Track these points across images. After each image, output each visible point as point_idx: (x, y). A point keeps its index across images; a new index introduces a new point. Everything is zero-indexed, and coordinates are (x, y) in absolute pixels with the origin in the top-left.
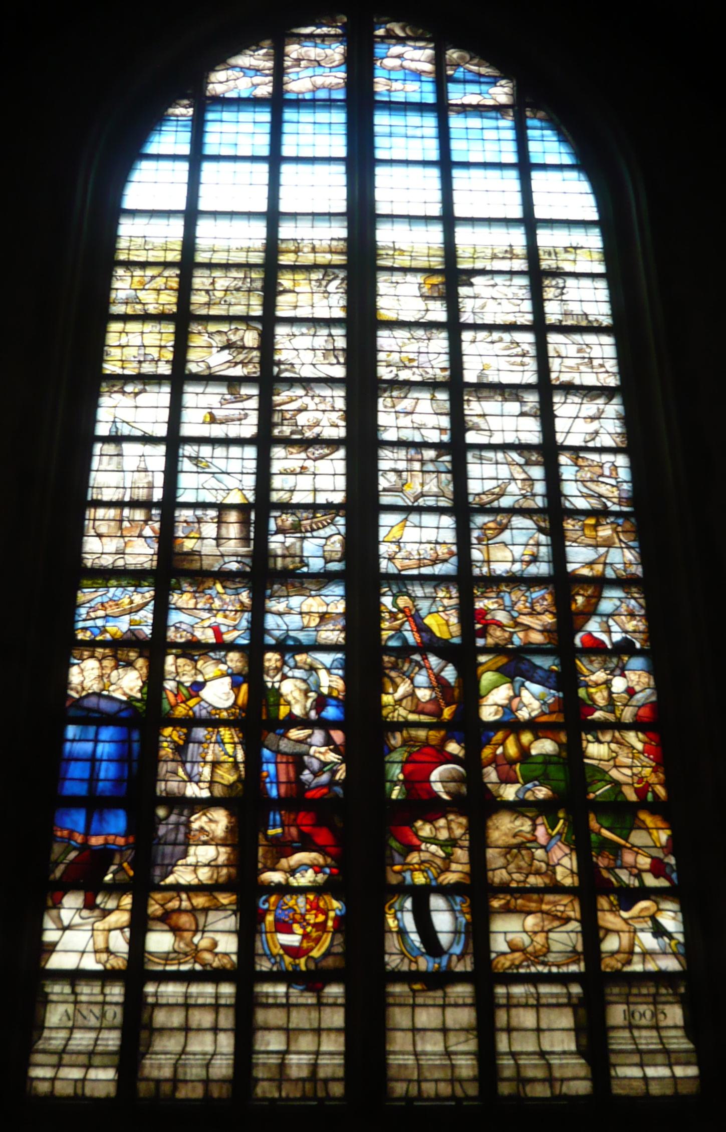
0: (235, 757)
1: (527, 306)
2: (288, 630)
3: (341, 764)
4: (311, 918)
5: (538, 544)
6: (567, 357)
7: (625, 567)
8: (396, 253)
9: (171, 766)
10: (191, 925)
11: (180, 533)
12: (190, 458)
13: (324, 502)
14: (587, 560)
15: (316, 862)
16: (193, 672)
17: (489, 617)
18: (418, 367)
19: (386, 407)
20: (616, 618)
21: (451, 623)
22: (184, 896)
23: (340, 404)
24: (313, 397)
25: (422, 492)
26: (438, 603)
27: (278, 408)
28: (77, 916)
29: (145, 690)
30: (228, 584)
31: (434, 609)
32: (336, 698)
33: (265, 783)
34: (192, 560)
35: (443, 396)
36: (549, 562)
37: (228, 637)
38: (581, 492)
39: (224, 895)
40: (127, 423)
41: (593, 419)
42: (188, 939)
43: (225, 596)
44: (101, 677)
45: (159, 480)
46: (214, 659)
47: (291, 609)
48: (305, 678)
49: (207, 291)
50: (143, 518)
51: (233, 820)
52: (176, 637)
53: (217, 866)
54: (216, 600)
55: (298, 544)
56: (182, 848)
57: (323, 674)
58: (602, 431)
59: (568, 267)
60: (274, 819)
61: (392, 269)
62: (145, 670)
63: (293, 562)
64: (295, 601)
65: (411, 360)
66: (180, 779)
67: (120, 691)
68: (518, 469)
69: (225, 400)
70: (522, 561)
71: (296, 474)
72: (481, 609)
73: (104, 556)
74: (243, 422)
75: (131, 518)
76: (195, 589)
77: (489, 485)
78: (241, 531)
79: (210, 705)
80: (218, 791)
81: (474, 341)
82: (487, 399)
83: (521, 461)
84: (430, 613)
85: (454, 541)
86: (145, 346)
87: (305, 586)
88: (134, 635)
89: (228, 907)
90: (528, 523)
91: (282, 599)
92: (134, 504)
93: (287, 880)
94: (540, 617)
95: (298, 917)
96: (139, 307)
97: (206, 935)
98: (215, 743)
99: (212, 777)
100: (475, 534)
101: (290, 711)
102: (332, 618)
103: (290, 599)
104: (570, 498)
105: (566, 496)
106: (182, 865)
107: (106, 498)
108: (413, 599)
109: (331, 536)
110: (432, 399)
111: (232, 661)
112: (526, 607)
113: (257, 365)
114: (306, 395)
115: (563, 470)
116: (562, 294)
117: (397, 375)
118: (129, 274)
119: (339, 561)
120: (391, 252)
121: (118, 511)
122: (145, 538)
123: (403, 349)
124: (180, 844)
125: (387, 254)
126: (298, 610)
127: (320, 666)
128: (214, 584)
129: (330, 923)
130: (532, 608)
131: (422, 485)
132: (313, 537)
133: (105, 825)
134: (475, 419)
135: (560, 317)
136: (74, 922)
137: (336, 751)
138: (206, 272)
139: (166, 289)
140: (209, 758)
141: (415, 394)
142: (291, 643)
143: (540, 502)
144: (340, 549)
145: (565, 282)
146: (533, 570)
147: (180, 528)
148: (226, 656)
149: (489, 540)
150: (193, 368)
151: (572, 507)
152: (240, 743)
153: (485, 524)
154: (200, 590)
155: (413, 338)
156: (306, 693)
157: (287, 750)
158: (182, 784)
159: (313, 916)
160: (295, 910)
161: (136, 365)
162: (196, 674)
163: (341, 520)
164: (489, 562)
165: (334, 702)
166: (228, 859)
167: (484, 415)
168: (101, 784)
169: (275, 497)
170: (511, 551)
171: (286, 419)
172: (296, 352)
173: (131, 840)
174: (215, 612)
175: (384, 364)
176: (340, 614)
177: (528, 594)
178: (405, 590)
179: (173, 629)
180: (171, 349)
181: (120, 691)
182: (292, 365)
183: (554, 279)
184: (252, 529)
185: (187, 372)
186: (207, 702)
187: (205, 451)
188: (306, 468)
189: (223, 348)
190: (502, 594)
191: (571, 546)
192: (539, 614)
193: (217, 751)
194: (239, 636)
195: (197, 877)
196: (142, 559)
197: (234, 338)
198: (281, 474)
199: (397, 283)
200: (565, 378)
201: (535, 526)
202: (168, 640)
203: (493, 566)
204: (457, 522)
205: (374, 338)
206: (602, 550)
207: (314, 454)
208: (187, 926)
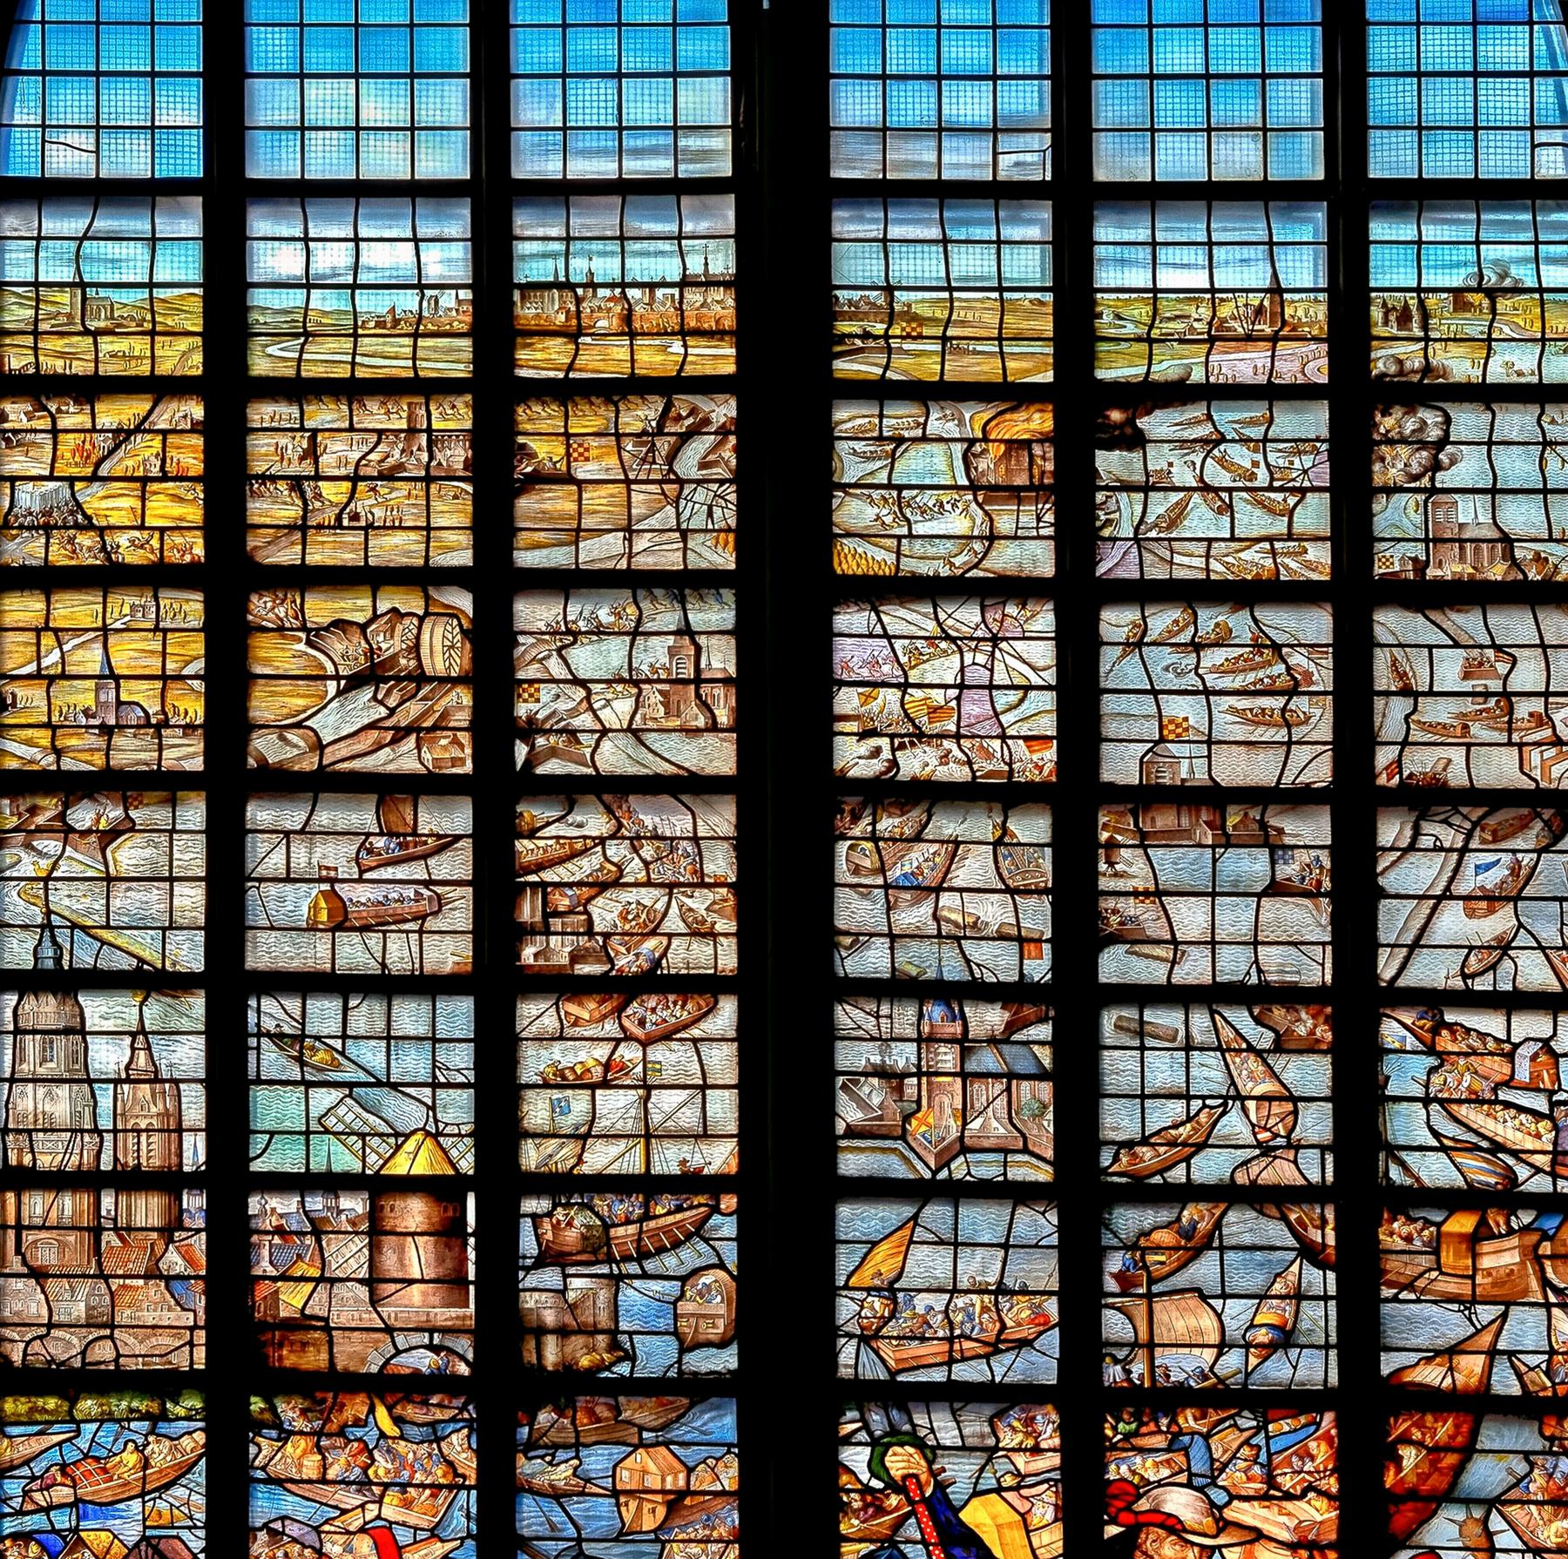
1: (1314, 514)
2: (579, 1540)
5: (1298, 1296)
6: (1431, 693)
7: (1549, 1362)
8: (895, 330)
11: (264, 1266)
12: (278, 1037)
13: (675, 1169)
14: (1441, 1343)
17: (1143, 1505)
18: (958, 737)
19: (856, 870)
20: (1508, 1510)
21: (1035, 1521)
23: (720, 863)
24: (635, 842)
25: (962, 1138)
26: (1001, 1465)
27: (533, 878)
30: (410, 1411)
31: (988, 1481)
34: (304, 1345)
35: (1033, 828)
36: (1327, 1347)
38: (1436, 1134)
40: (84, 928)
41: (1492, 900)
43: (402, 1447)
45: (194, 1106)
47: (588, 1481)
49: (296, 483)
50: (155, 1221)
54: (376, 1454)
55: (604, 1295)
58: (1523, 939)
59: (1460, 366)
61: (880, 391)
64: (597, 1460)
65: (935, 711)
68: (1253, 1063)
69: (370, 851)
70: (1247, 1346)
71: (593, 1087)
72: (1123, 1480)
73: (55, 1333)
74: (431, 924)
75: (122, 1222)
76: (317, 1424)
77: (1165, 1114)
78: (440, 1260)
81: (1136, 644)
82: (1171, 838)
83: (1265, 1039)
84: (976, 1494)
85: (1055, 1286)
86: (117, 678)
88: (156, 1550)
90: (1277, 1232)
91: (561, 1455)
92: (130, 1180)
94: (1289, 1505)
96: (86, 540)
100: (1115, 1263)
102: (700, 1507)
103: (583, 1452)
104: (1403, 1155)
105: (1393, 1151)
107: (45, 1162)
108: (931, 1452)
109: (696, 1272)
110: (998, 843)
112: (1249, 1479)
113: (465, 738)
114: (613, 837)
115: (1390, 1065)
116: (1436, 466)
117: (894, 763)
118: (45, 423)
119: (722, 1344)
120: (879, 329)
121: (85, 1200)
122: (168, 1279)
123: (914, 677)
125: (866, 336)
126: (608, 1483)
128: (372, 1410)
130: (1270, 1481)
131: (964, 1116)
132: (645, 1276)
134: (1130, 907)
135: (1418, 550)
138: (285, 412)
139: (165, 478)
141: (947, 825)
143: (1314, 1169)
144: (722, 1310)
145: (1448, 421)
146: (1278, 1371)
147: (265, 1252)
149: (1152, 1281)
150: (266, 747)
151: (1409, 1181)
153: (1146, 1234)
155: (948, 638)
161: (94, 740)
163: (727, 1227)
164: (1151, 1346)
167: (1158, 894)
169: (531, 1156)
170: (1219, 1316)
171: (557, 914)
172: (582, 693)
174: (377, 1490)
175: (852, 727)
176: (723, 1493)
177: (1260, 1440)
178: (907, 1427)
179: (263, 1536)
180: (198, 685)
182: (572, 734)
183: (1411, 410)
184: (471, 1254)
185: (252, 762)
187: (324, 1013)
188: (622, 1067)
189: (355, 682)
190: (1186, 1439)
191: (1395, 1299)
192: (1288, 1496)
196: (166, 1341)
197: (390, 644)
198: (546, 1085)
199: (900, 440)
200: (1420, 762)
201: (1292, 1242)
203: (1163, 1357)
204: (1061, 1229)
205: (826, 637)
206: (1486, 1313)
207: (642, 1023)
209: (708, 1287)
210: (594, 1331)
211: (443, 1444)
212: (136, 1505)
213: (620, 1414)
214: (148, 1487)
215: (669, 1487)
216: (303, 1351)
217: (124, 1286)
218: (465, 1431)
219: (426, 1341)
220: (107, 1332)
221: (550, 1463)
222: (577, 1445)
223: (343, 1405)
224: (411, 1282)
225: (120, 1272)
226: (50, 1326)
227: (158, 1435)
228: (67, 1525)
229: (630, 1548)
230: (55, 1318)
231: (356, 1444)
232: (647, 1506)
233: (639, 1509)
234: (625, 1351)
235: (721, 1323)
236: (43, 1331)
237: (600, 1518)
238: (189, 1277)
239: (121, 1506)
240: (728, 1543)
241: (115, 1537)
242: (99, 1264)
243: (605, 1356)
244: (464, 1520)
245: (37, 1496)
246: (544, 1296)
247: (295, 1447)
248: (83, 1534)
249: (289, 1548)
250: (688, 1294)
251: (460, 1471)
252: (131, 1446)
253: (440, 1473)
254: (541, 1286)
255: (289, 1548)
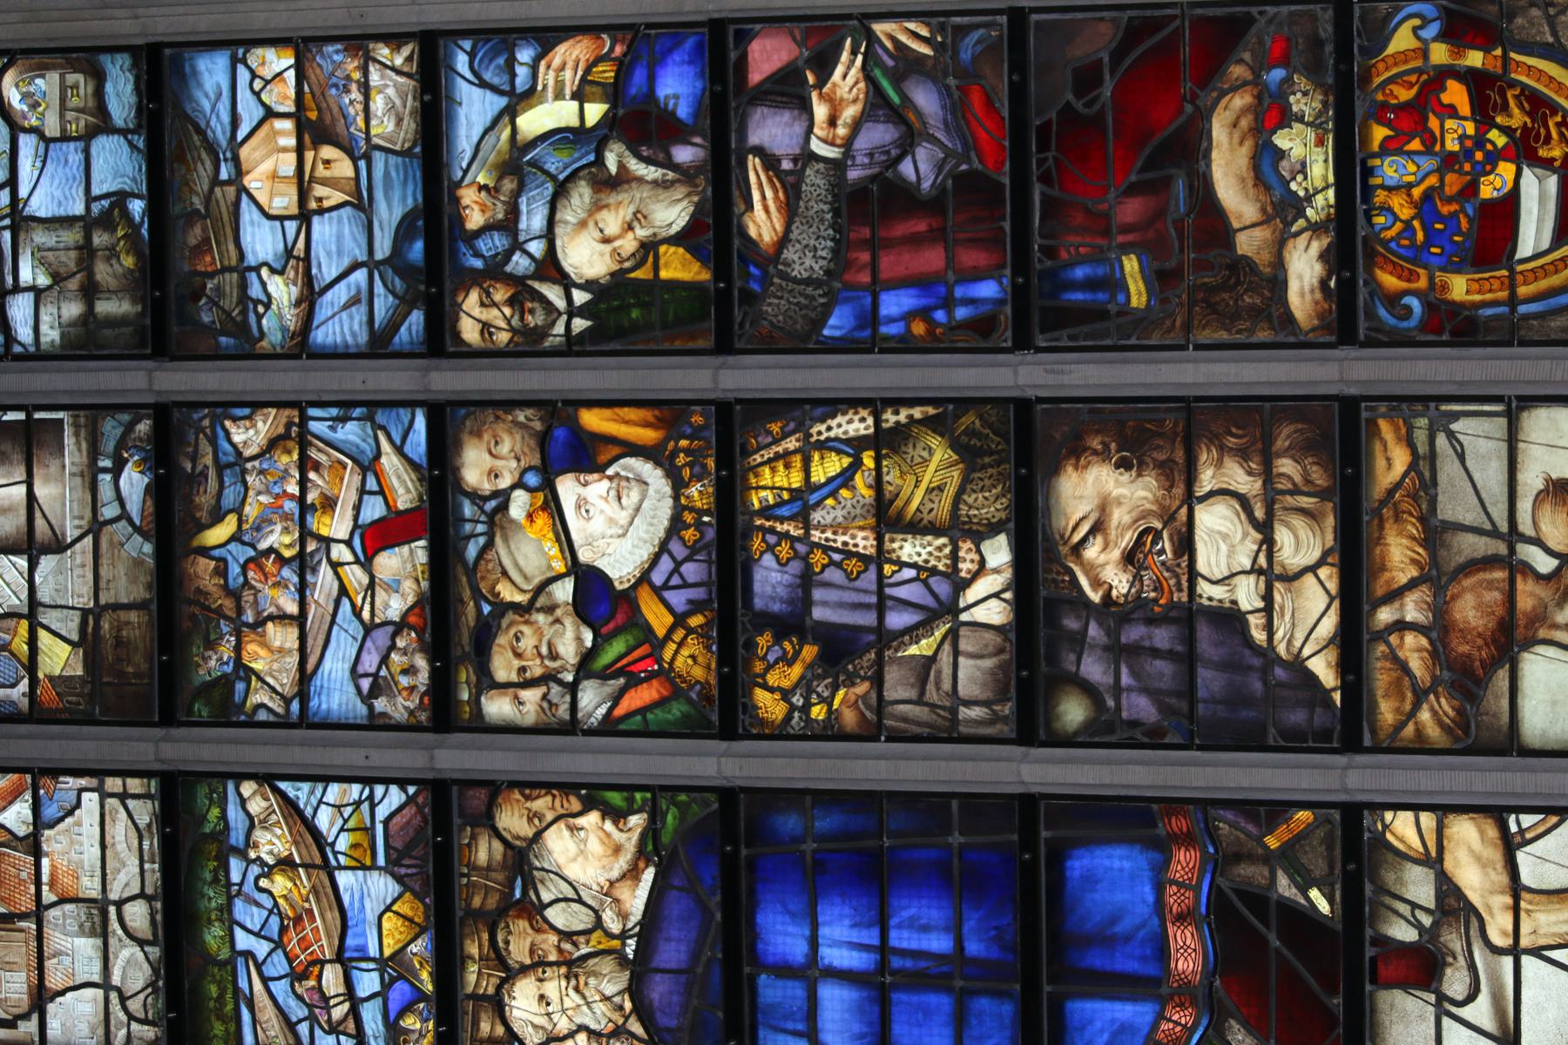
0: (856, 445)
2: (371, 264)
3: (871, 38)
4: (1454, 133)
9: (897, 686)
10: (1490, 585)
15: (1245, 123)
16: (541, 618)
22: (1385, 615)
28: (1466, 1012)
29: (615, 798)
30: (205, 500)
32: (624, 68)
33: (955, 327)
34: (119, 642)
37: (405, 492)
39: (1380, 463)
42: (1543, 592)
43: (251, 511)
44: (572, 967)
46: (490, 544)
47: (289, 252)
48: (549, 188)
51: (1096, 443)
52: (412, 689)
53: (1271, 496)
54: (263, 545)
55: (41, 237)
56: (1204, 632)
57: (534, 121)
60: (1091, 284)
62: (541, 804)
63: (112, 253)
64: (261, 241)
66: (947, 647)
67: (623, 892)
73: (116, 979)
76: (225, 627)
79: (663, 548)
80: (988, 504)
87: (198, 203)
89: (1422, 449)
91: (255, 291)
93: (1316, 228)
95: (1453, 182)
97: (1525, 526)
98: (807, 526)
99: (934, 530)
101: (677, 240)
102: (320, 97)
103: (251, 260)
106: (1269, 628)
111: (494, 474)
119: (99, 77)
122: (39, 822)
124: (1190, 640)
126: (291, 226)
127: (506, 134)
128: (205, 551)
129: (1475, 59)
133: (1120, 928)
136: (1488, 1024)
137: (824, 64)
140: (864, 542)
142: (417, 250)
144: (54, 77)
148: (476, 497)
152: (802, 428)
154: (228, 604)
156: (608, 184)
157: (825, 248)
158: (964, 645)
159: (1450, 124)
160: (1428, 196)
162: (550, 609)
165: (639, 77)
166: (1243, 455)
168: (973, 947)
173: (1179, 824)
176: (299, 67)
179: (380, 704)
181: (623, 892)
186: (655, 560)
193: (839, 514)
194: (399, 450)
195: (1312, 569)
196: (120, 830)
202: (423, 717)
208: (1495, 596)
209: (25, 96)
210: (86, 251)
211: (248, 453)
212: (343, 879)
213: (198, 211)
214: (318, 861)
215: (291, 142)
216: (129, 642)
217: (52, 884)
218: (227, 423)
219: (108, 477)
220: (112, 909)
221: (268, 306)
222: (243, 270)
223: (199, 591)
224: (31, 496)
225: (32, 889)
226: (105, 985)
227: (247, 845)
228: (375, 975)
229: (379, 194)
230: (96, 978)
231: (251, 574)
232: (321, 171)
233: (325, 182)
234: (112, 205)
235: (72, 78)
236: (114, 996)
237: (340, 238)
238: (36, 798)
239: (346, 899)
240: (368, 59)
241: (388, 909)
242: (24, 916)
243: (120, 233)
244: (350, 426)
245: (338, 1013)
246: (45, 318)
247: (256, 658)
248: (387, 952)
249: (396, 669)
250: (34, 122)
251: (281, 430)
252: (263, 883)
253: (285, 459)
254: (31, 322)
255: (396, 669)
